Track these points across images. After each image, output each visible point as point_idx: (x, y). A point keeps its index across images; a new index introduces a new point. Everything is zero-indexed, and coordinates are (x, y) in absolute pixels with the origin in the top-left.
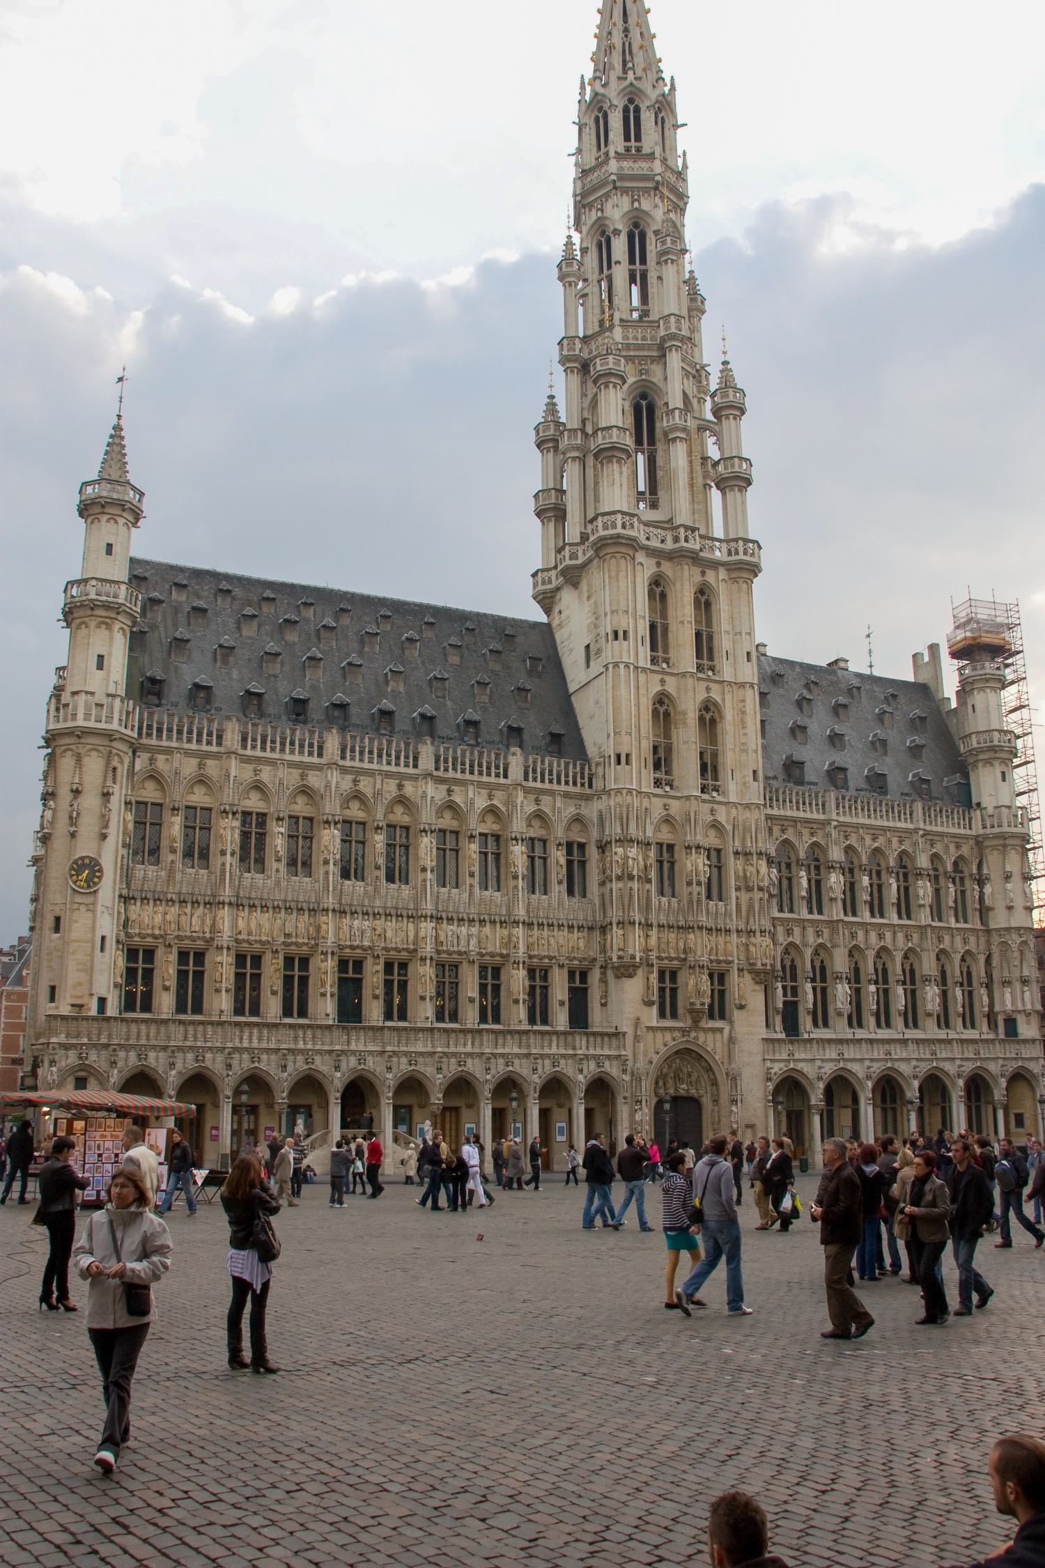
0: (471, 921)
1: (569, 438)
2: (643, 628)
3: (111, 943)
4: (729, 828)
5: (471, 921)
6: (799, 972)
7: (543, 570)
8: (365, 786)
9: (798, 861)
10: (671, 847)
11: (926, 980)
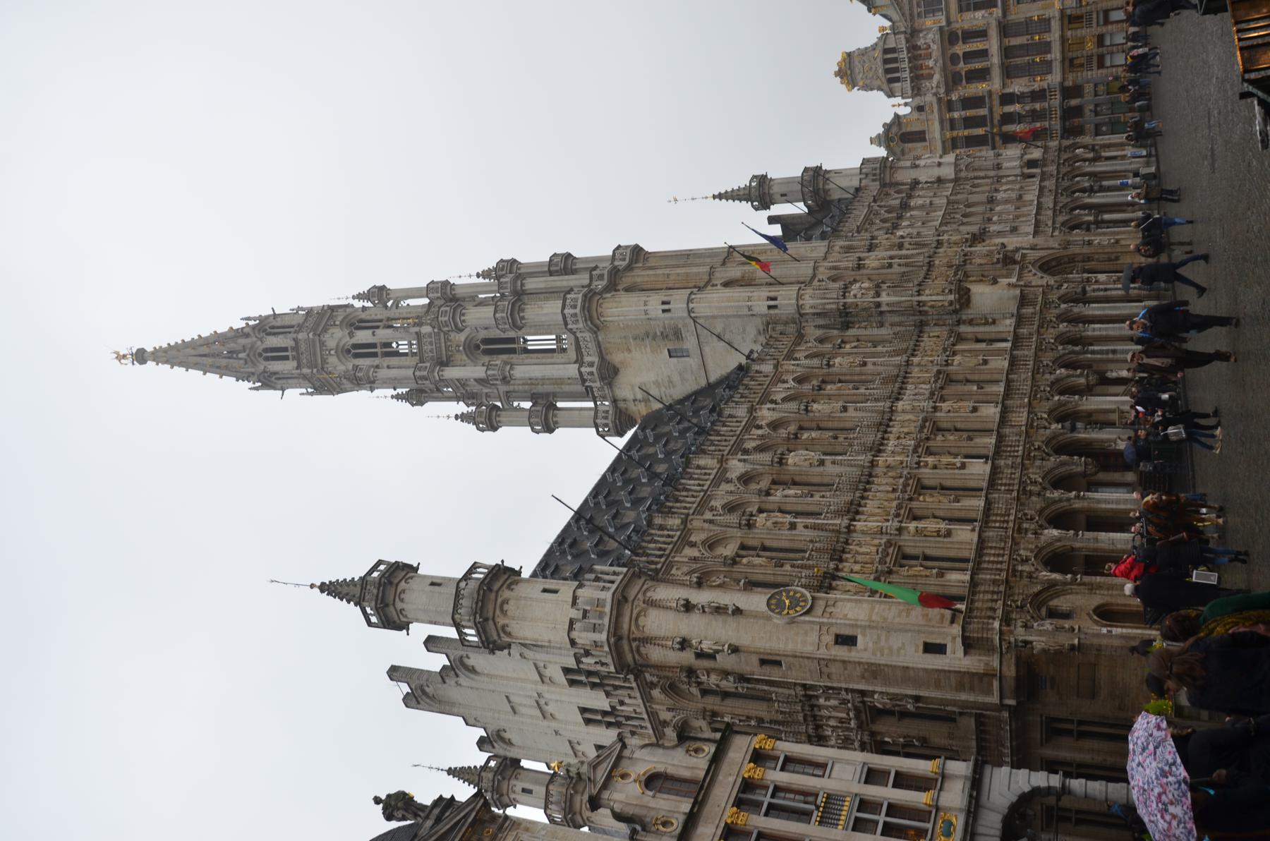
1: (493, 370)
7: (596, 417)
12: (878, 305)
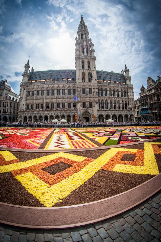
2: (81, 66)
3: (24, 104)
5: (61, 99)
8: (50, 86)
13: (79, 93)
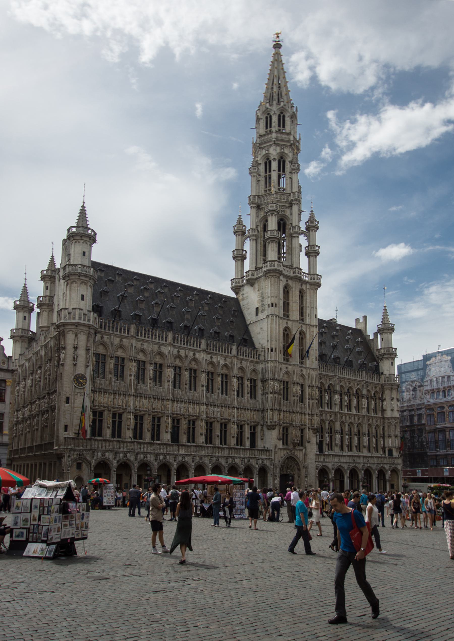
0: (218, 406)
1: (252, 231)
3: (88, 409)
4: (307, 377)
5: (218, 406)
6: (324, 430)
8: (182, 353)
9: (325, 390)
10: (287, 382)
11: (364, 434)
12: (268, 394)
13: (277, 396)
